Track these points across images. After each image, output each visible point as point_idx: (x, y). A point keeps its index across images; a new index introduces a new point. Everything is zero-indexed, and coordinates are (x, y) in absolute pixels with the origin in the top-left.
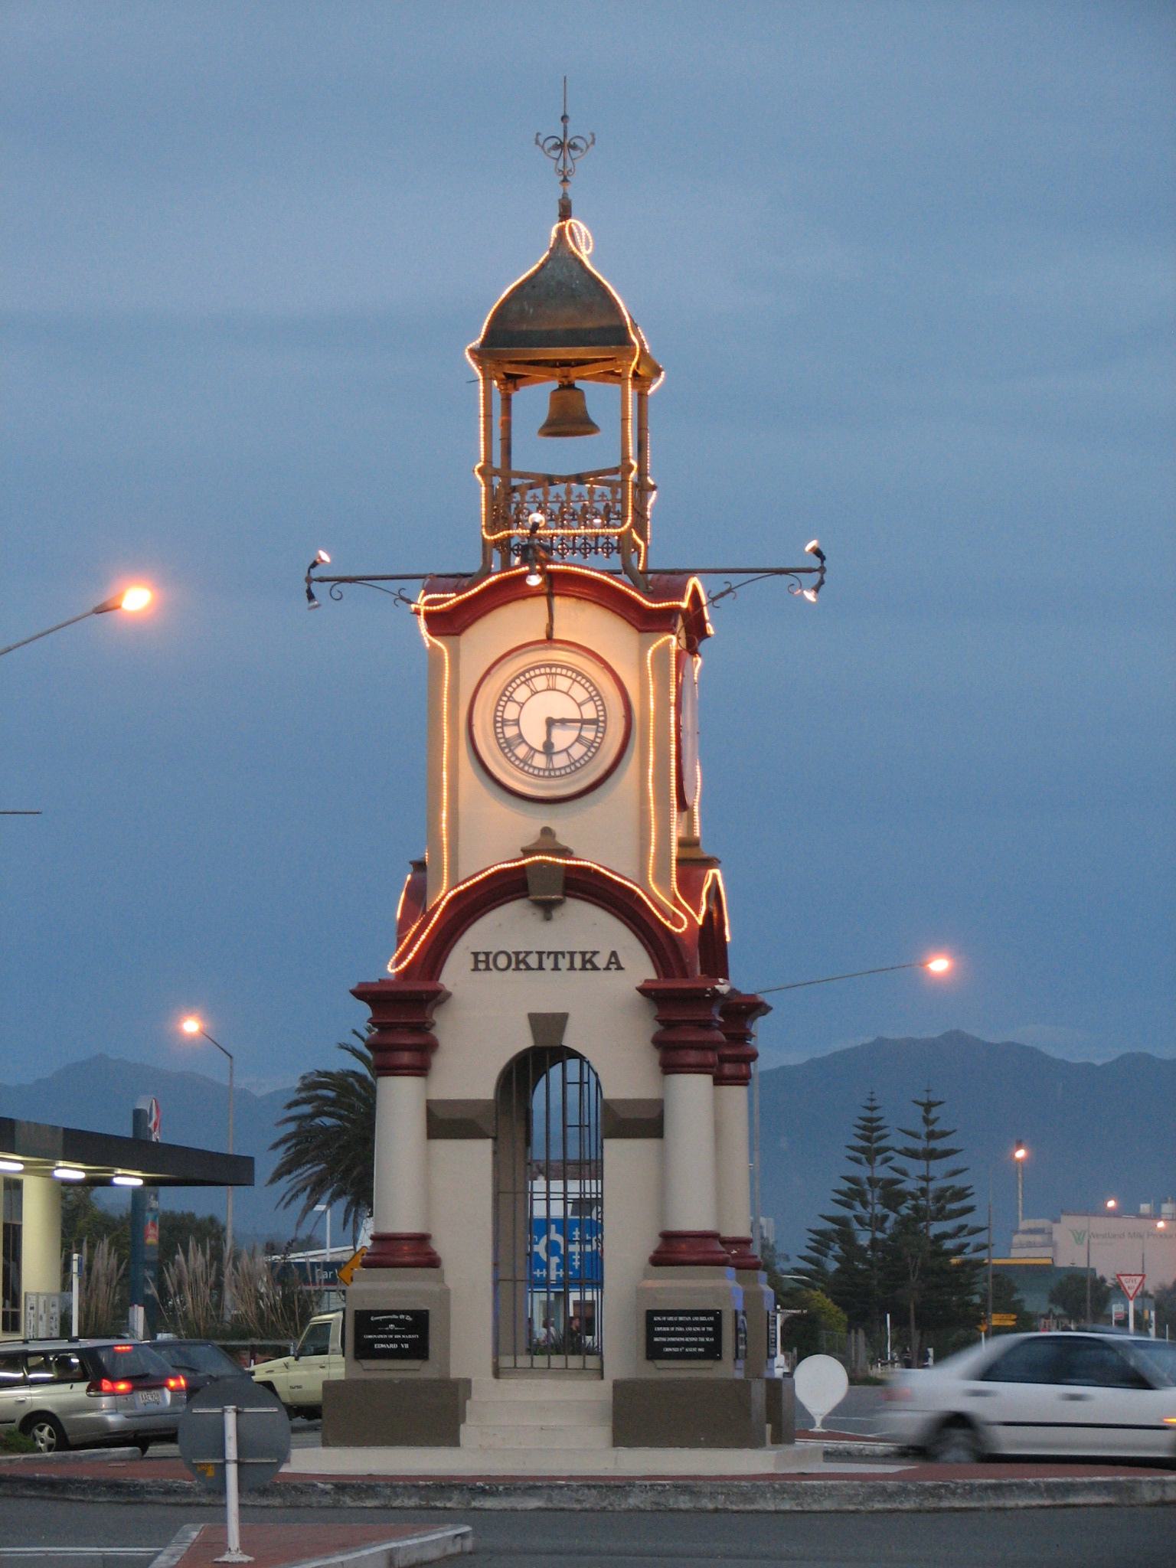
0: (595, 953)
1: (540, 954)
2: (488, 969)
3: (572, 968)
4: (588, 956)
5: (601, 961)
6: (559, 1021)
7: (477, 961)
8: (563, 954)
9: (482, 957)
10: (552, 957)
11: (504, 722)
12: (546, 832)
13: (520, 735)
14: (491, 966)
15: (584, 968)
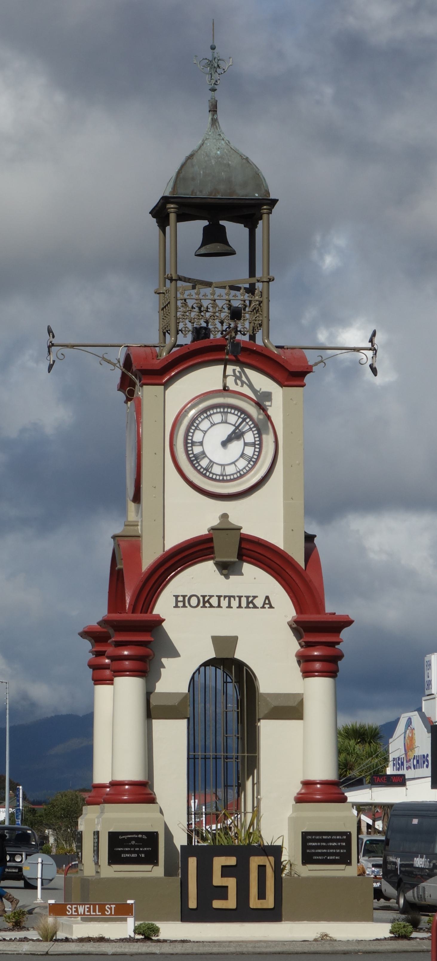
0: (255, 597)
1: (219, 597)
2: (184, 606)
3: (240, 606)
4: (250, 599)
5: (259, 602)
6: (233, 641)
7: (177, 601)
8: (234, 597)
9: (180, 599)
10: (227, 599)
11: (193, 443)
12: (225, 516)
13: (203, 453)
14: (187, 604)
15: (247, 607)
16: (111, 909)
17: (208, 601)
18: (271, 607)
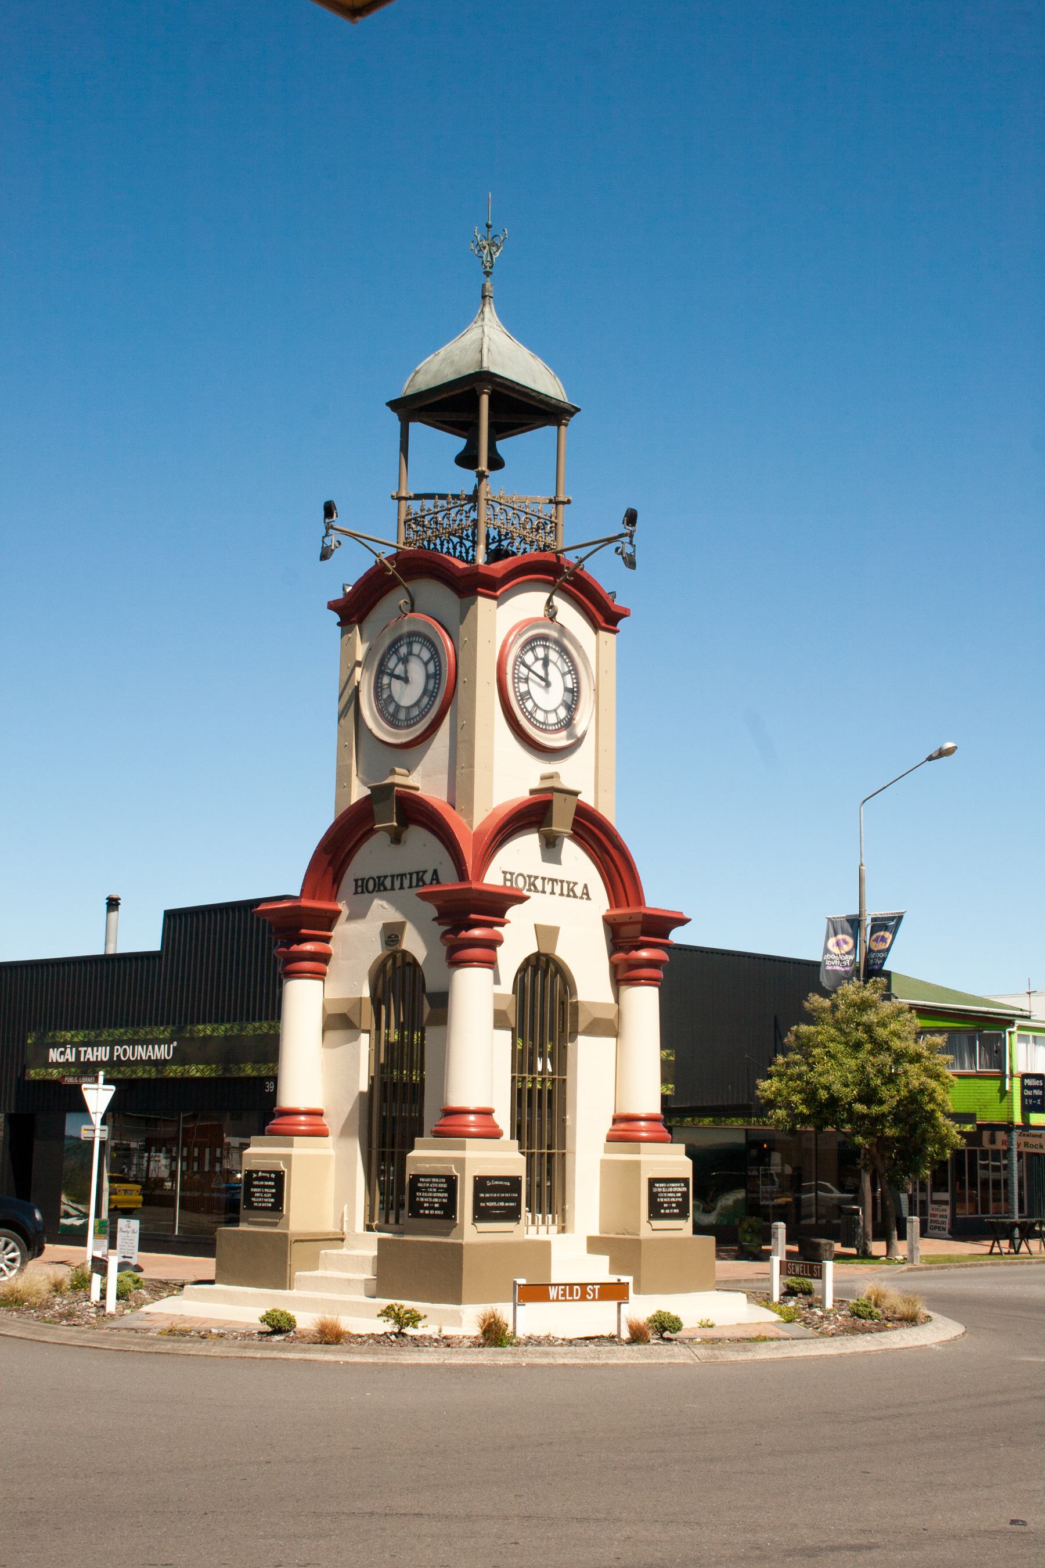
0: (425, 872)
1: (393, 876)
2: (362, 892)
7: (357, 886)
8: (405, 875)
9: (360, 883)
16: (594, 1291)
17: (383, 884)
18: (588, 898)
